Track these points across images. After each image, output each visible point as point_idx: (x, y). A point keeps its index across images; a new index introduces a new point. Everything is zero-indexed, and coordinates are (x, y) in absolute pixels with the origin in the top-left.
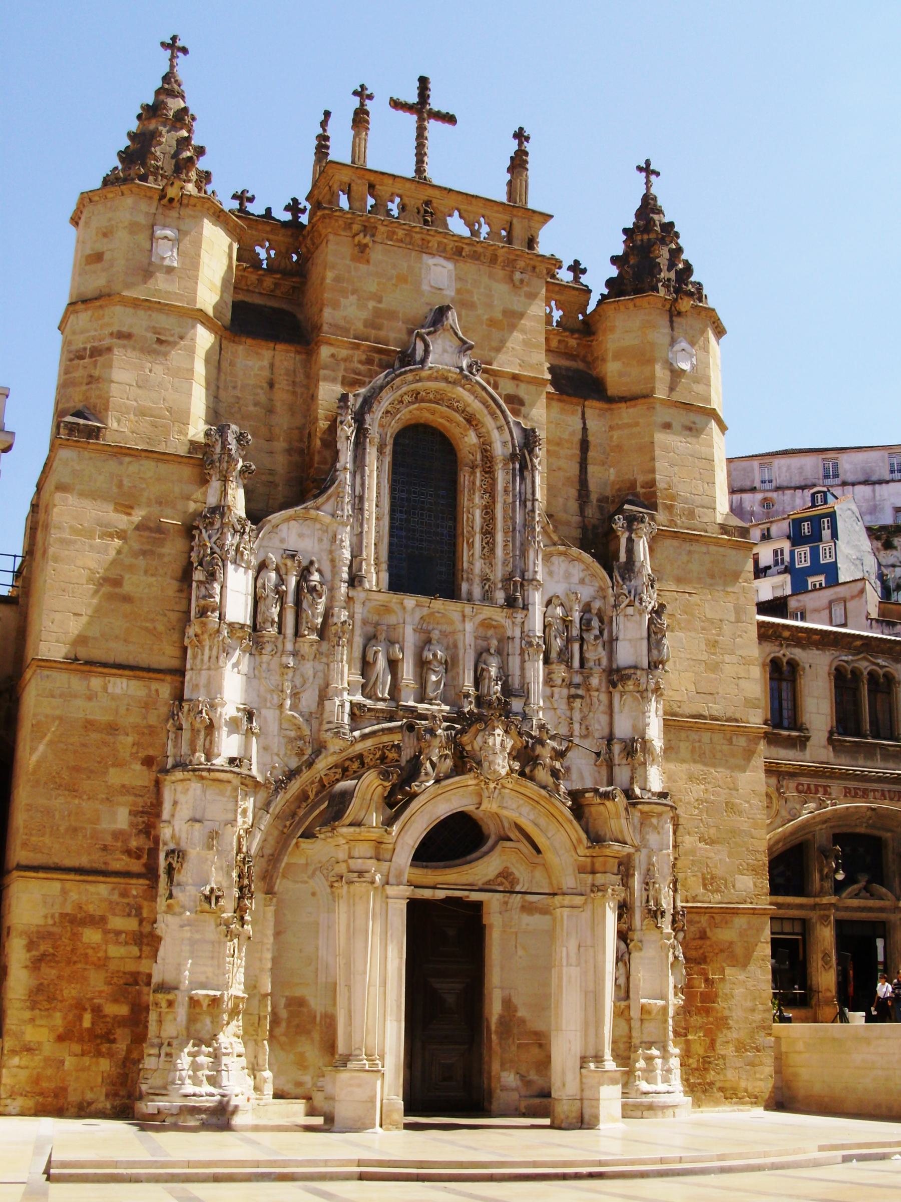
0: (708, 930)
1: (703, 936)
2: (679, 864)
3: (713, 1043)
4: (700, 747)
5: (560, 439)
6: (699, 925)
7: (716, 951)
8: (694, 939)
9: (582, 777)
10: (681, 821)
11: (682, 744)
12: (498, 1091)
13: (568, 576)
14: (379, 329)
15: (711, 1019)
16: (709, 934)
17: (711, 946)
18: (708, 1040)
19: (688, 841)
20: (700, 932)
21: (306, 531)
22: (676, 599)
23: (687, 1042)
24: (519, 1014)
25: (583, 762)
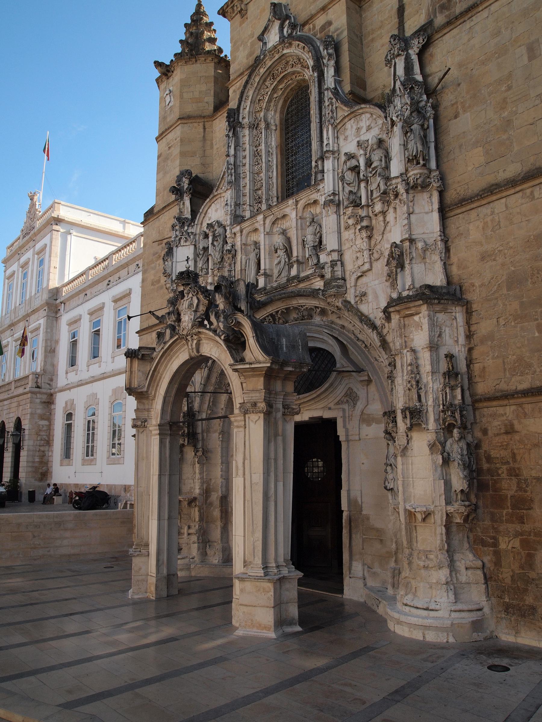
0: (516, 422)
1: (510, 430)
2: (476, 354)
3: (530, 556)
4: (493, 220)
5: (382, 22)
6: (505, 418)
7: (529, 446)
8: (498, 435)
9: (376, 297)
10: (475, 307)
11: (471, 227)
12: (348, 578)
13: (358, 129)
14: (253, 53)
15: (527, 527)
16: (517, 426)
17: (521, 441)
18: (523, 553)
19: (483, 328)
20: (506, 425)
21: (218, 206)
22: (459, 85)
23: (497, 554)
24: (364, 512)
25: (377, 282)
